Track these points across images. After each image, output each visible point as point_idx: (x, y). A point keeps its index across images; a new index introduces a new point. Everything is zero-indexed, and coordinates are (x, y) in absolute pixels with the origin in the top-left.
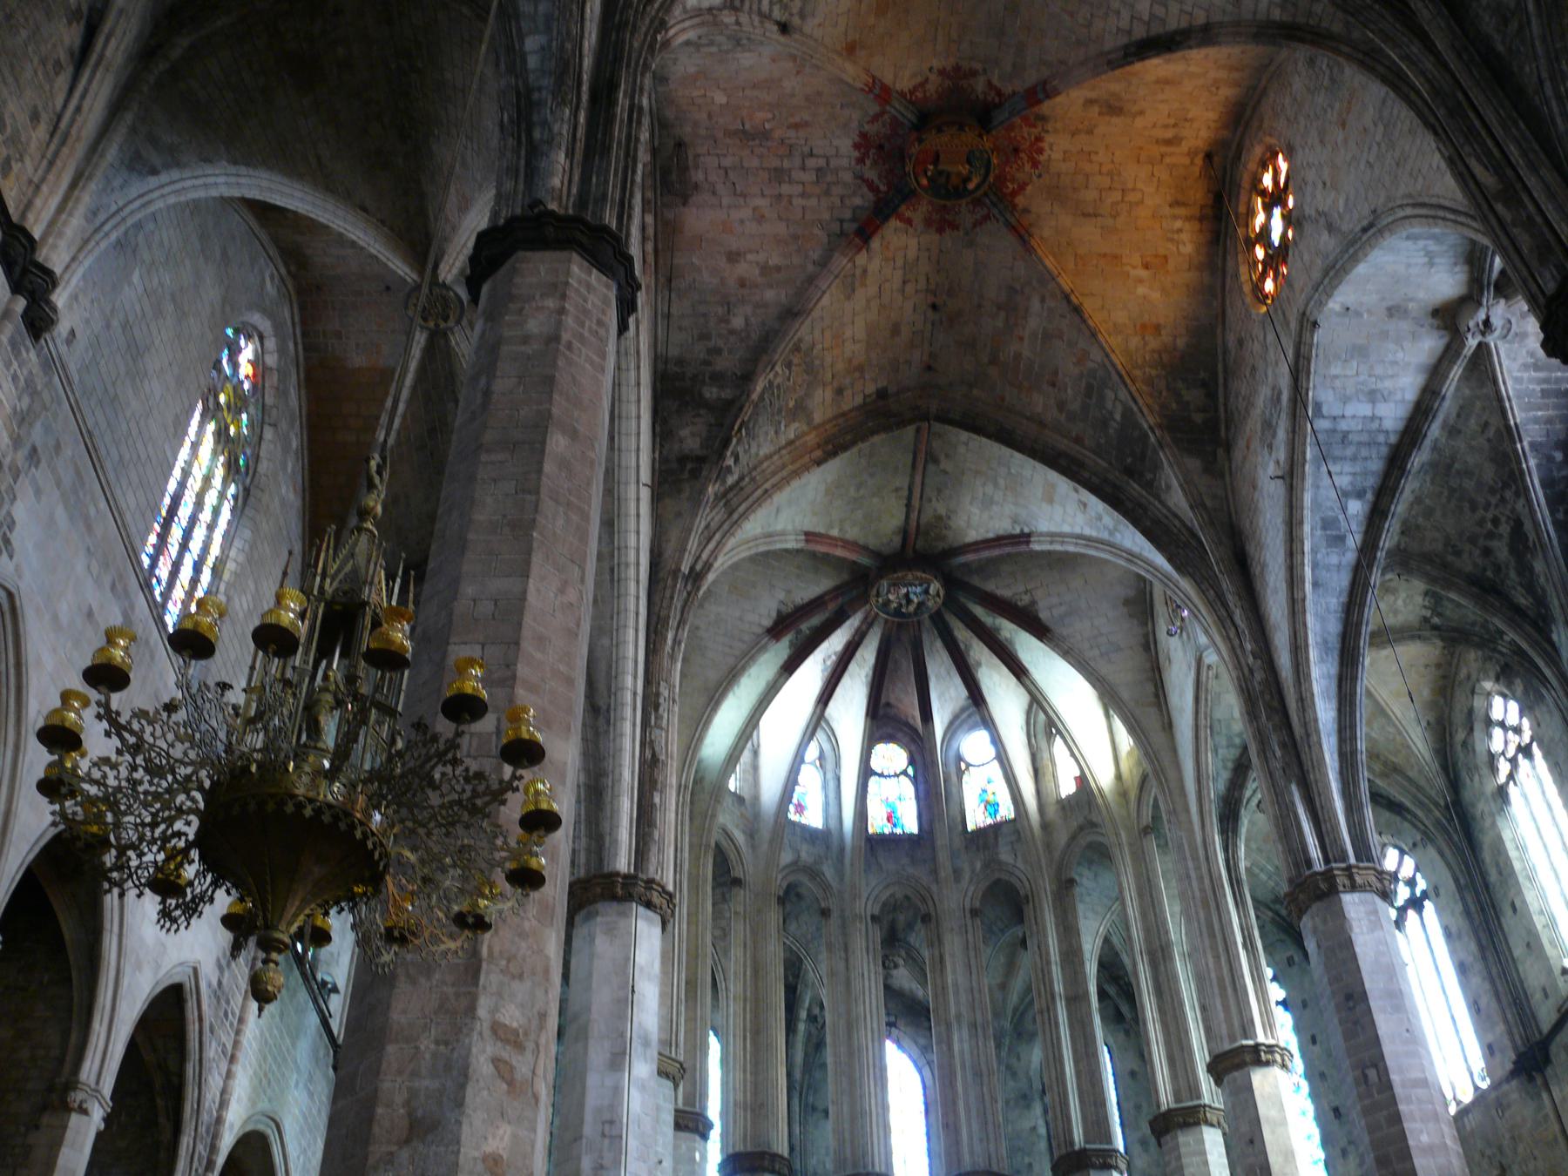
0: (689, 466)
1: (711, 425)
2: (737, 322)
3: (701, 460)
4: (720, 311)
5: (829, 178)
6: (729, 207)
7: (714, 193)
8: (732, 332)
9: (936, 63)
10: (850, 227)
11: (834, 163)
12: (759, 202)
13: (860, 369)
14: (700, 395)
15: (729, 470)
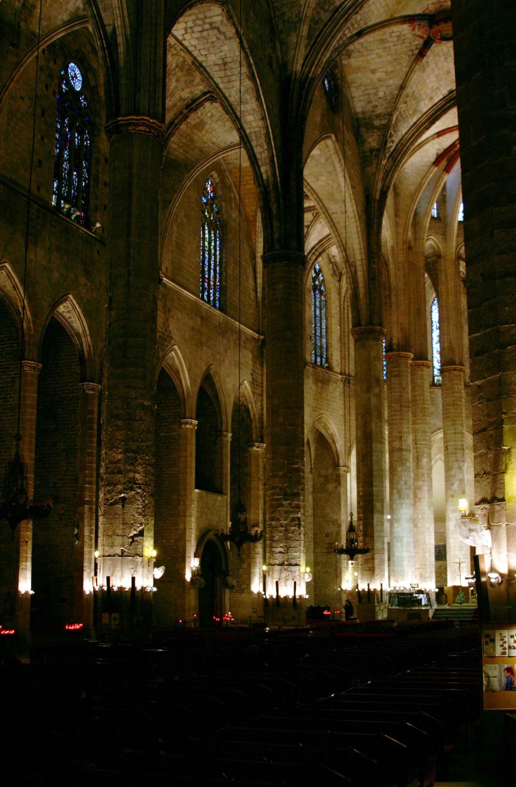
0: (374, 154)
1: (379, 136)
2: (381, 94)
3: (378, 150)
4: (374, 91)
5: (403, 38)
6: (367, 55)
7: (360, 52)
8: (380, 98)
9: (430, 3)
10: (416, 52)
11: (403, 33)
12: (378, 51)
13: (438, 88)
14: (373, 124)
15: (391, 147)
